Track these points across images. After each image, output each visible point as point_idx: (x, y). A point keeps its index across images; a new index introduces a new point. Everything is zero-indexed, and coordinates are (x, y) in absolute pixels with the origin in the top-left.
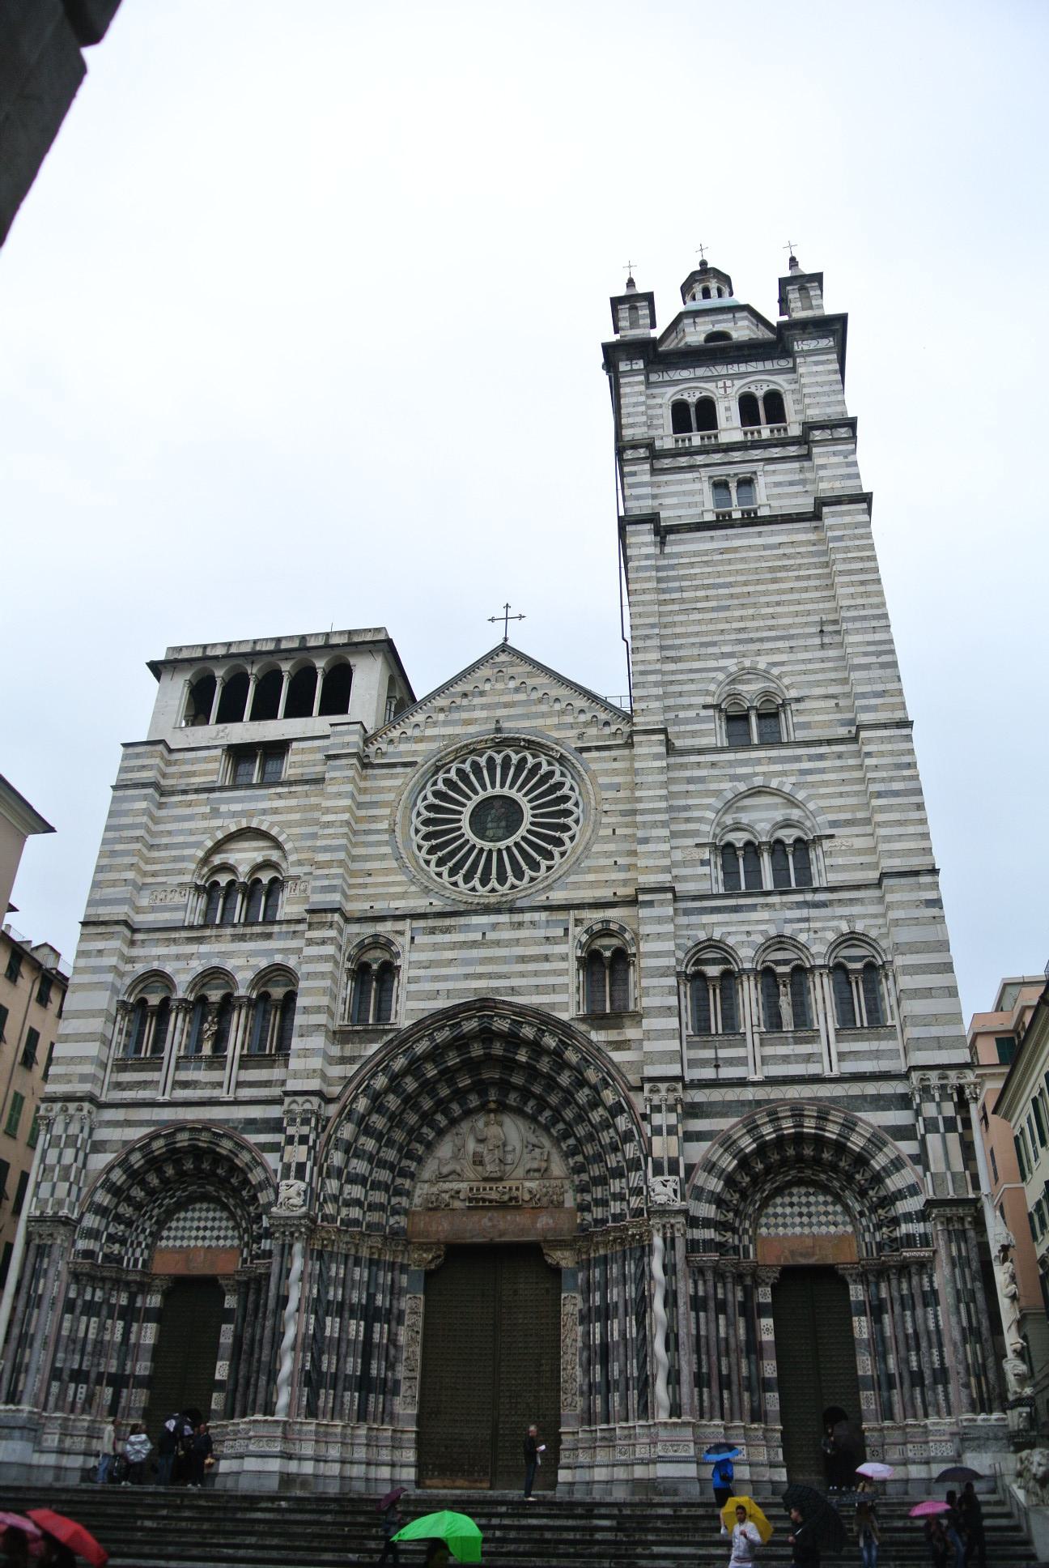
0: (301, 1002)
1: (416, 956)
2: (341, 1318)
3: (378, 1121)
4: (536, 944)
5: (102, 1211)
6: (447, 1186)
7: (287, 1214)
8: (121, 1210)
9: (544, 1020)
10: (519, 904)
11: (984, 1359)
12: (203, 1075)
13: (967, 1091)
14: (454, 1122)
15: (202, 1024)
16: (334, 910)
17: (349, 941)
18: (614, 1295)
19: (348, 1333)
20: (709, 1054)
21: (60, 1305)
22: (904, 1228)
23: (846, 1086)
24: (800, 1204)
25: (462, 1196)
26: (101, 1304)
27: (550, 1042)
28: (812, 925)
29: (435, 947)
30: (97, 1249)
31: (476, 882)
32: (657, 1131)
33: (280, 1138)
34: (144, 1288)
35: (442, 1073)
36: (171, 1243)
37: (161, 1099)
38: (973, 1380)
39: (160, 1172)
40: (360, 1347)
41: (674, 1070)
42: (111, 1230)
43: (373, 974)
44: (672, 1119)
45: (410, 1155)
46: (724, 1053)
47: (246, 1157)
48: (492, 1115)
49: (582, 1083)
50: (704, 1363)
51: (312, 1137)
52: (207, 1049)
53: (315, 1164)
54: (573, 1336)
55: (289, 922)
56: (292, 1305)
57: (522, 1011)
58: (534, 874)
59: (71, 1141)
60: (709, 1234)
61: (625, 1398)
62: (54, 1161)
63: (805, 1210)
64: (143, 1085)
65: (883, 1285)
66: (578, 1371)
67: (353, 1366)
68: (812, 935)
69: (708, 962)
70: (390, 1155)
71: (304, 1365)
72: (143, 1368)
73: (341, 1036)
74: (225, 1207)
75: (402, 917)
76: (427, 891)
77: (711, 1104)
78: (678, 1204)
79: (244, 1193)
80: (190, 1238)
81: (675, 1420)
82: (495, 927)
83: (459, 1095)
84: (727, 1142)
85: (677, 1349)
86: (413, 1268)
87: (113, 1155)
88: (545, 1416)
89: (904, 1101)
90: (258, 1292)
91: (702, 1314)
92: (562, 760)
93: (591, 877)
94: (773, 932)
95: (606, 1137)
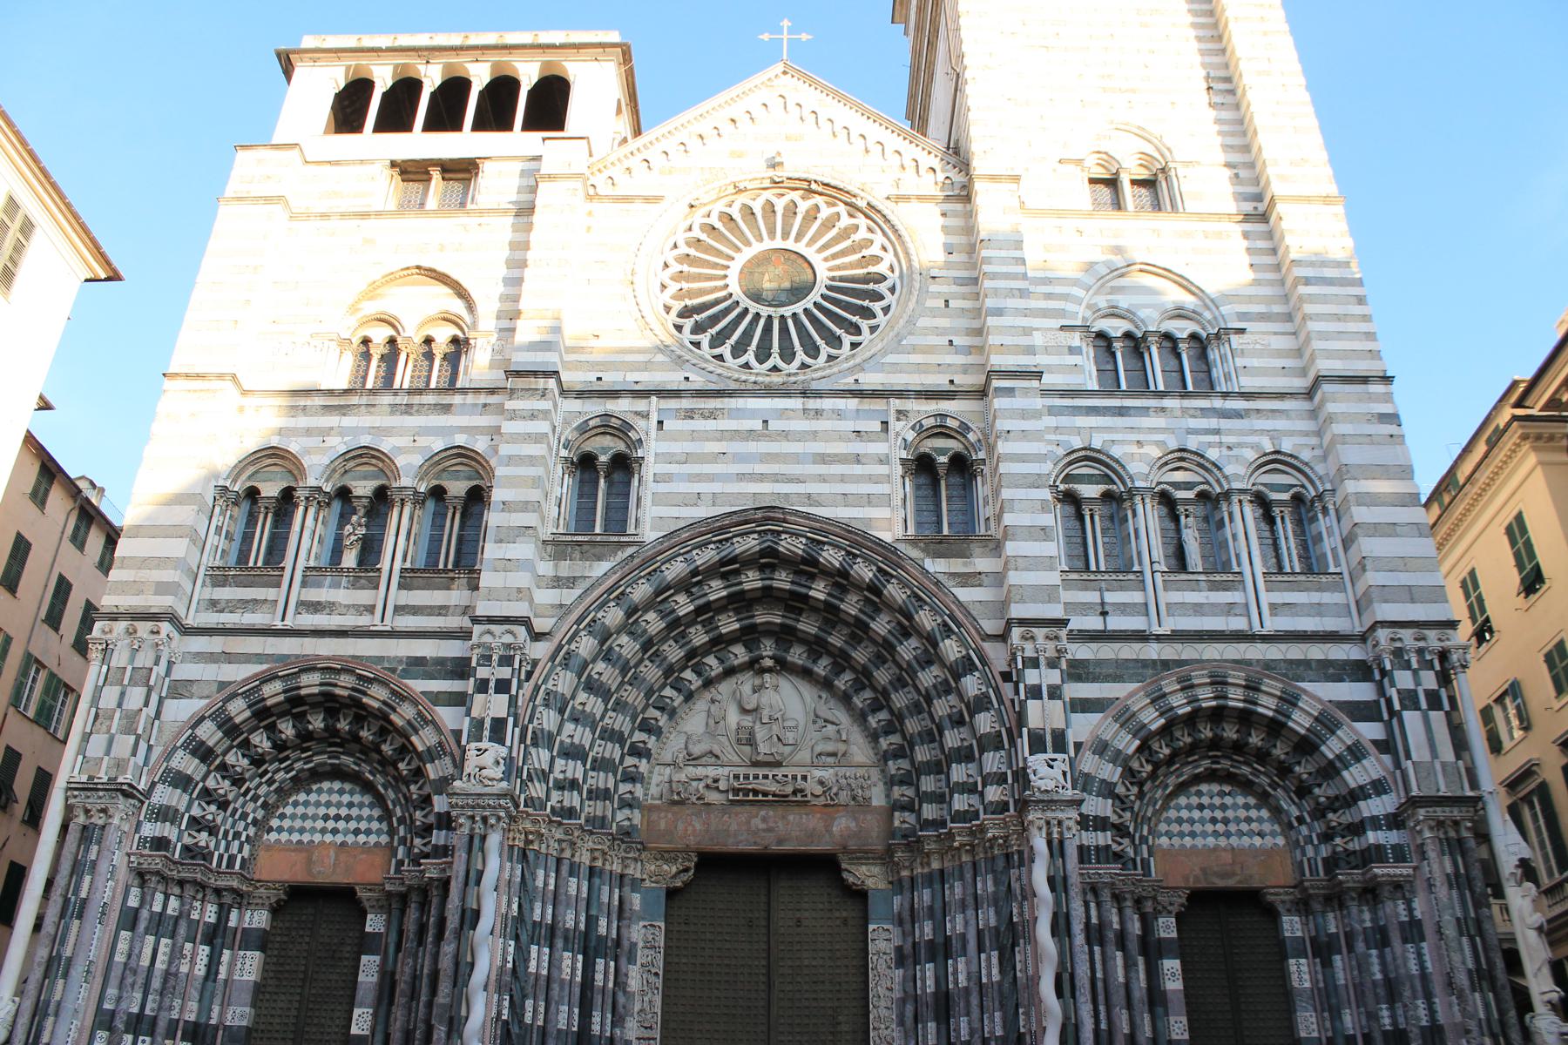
0: (497, 495)
2: (551, 947)
4: (840, 439)
5: (181, 781)
6: (700, 771)
7: (479, 789)
8: (211, 783)
9: (857, 541)
10: (814, 386)
11: (1502, 1012)
12: (343, 596)
13: (1454, 657)
14: (708, 683)
15: (341, 526)
16: (547, 374)
17: (566, 422)
18: (956, 924)
19: (560, 968)
20: (1092, 597)
21: (114, 916)
22: (1372, 837)
23: (1283, 646)
24: (1212, 807)
25: (722, 785)
26: (177, 919)
27: (864, 572)
28: (1225, 439)
29: (693, 436)
30: (174, 838)
31: (750, 357)
32: (1035, 692)
33: (469, 686)
34: (241, 899)
35: (699, 611)
36: (284, 836)
37: (279, 625)
39: (272, 729)
40: (577, 991)
41: (1056, 612)
42: (196, 811)
43: (604, 470)
44: (1054, 677)
45: (647, 727)
46: (1111, 597)
47: (407, 711)
48: (767, 676)
49: (907, 629)
50: (1103, 1016)
51: (515, 681)
52: (350, 559)
53: (515, 725)
54: (885, 983)
55: (477, 390)
57: (824, 531)
58: (833, 352)
59: (142, 677)
60: (1103, 838)
62: (113, 704)
63: (1218, 814)
64: (254, 604)
65: (1331, 916)
68: (1225, 451)
70: (621, 722)
71: (499, 1013)
73: (558, 548)
74: (368, 787)
75: (645, 394)
76: (679, 361)
77: (1099, 663)
78: (1069, 793)
79: (401, 766)
82: (783, 414)
83: (719, 643)
84: (1126, 718)
85: (1073, 996)
86: (647, 884)
87: (204, 702)
89: (1360, 671)
90: (424, 906)
91: (1097, 949)
92: (871, 212)
94: (1173, 444)
95: (941, 707)
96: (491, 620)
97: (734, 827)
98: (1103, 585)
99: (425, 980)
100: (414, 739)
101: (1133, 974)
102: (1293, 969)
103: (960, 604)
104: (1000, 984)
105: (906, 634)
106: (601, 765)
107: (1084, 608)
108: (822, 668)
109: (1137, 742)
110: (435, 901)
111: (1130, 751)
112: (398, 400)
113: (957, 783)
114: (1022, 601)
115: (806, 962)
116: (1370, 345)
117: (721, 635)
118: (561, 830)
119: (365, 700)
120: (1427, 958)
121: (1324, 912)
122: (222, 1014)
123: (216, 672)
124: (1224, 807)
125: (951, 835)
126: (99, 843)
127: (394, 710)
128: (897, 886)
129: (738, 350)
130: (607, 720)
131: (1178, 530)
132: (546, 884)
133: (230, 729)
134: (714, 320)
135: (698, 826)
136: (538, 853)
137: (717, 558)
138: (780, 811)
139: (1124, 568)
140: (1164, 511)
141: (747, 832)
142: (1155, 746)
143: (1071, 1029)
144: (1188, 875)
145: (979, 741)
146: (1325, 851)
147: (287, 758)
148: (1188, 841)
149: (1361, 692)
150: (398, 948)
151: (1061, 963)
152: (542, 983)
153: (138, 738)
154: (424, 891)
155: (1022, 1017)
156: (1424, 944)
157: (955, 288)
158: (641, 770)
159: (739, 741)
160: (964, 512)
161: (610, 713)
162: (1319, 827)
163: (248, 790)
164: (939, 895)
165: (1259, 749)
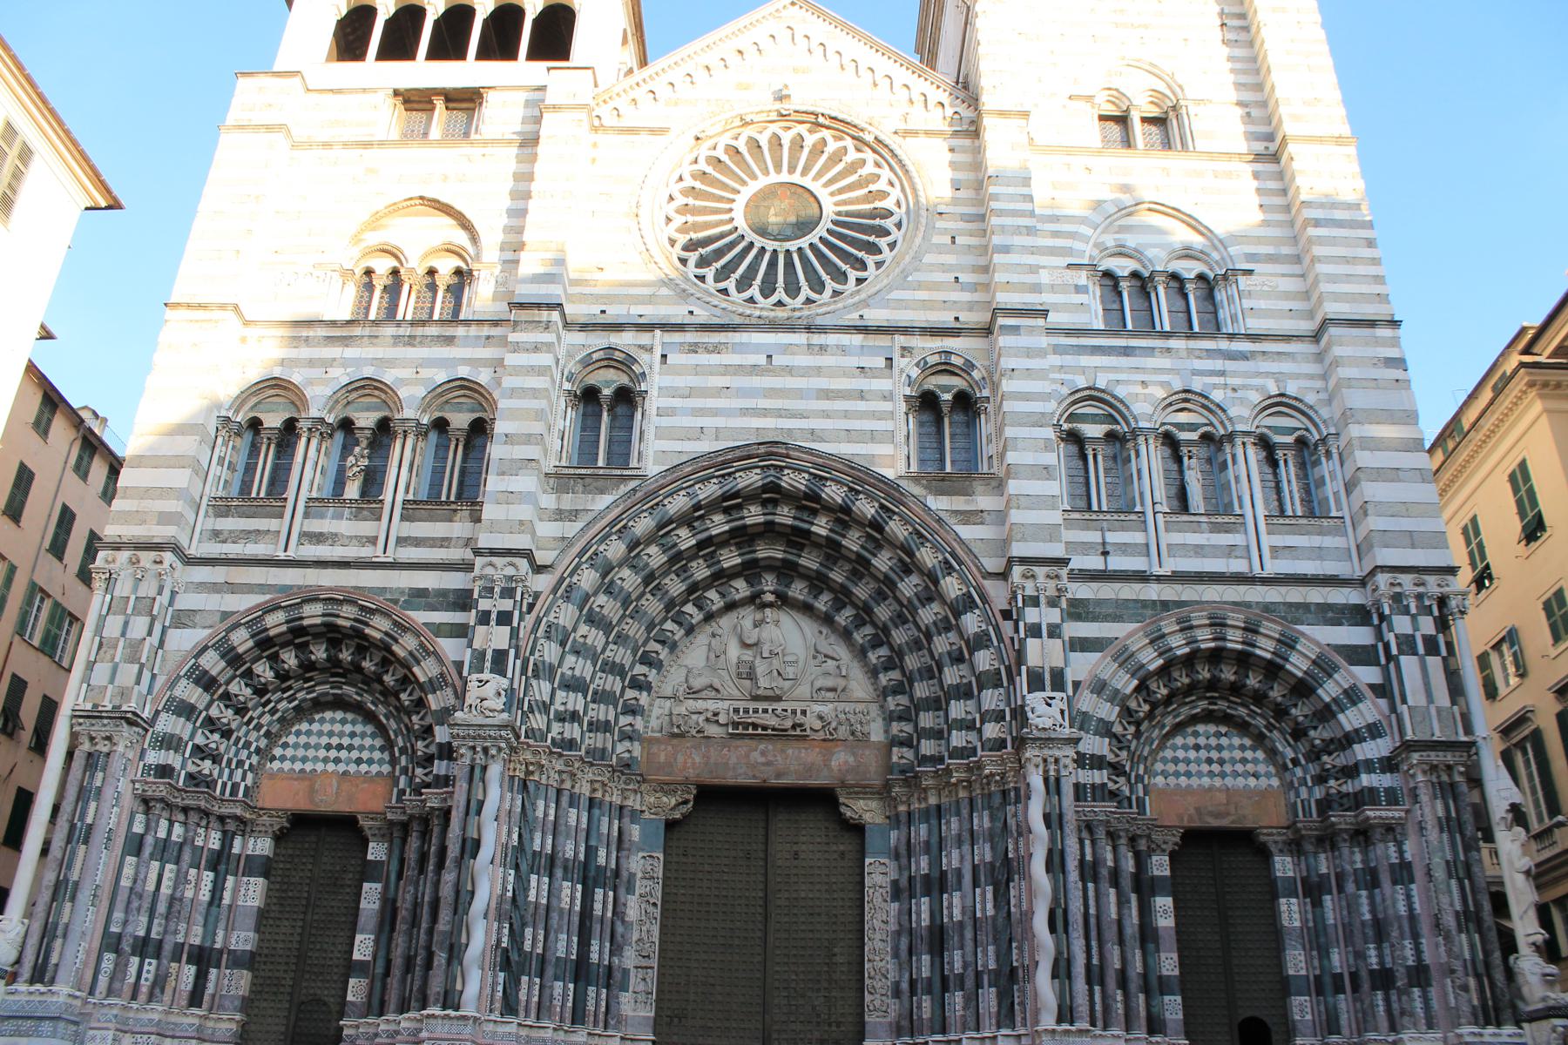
0: (500, 427)
1: (668, 381)
2: (551, 876)
3: (606, 605)
5: (185, 710)
6: (700, 705)
7: (480, 720)
9: (860, 478)
10: (819, 321)
11: (1486, 953)
12: (345, 527)
14: (709, 617)
15: (343, 458)
16: (551, 307)
17: (570, 355)
20: (1094, 537)
21: (119, 841)
22: (1366, 780)
23: (1283, 589)
24: (1208, 748)
25: (722, 719)
26: (181, 845)
28: (1230, 381)
29: (697, 370)
30: (177, 766)
31: (754, 291)
32: (1035, 631)
33: (471, 617)
34: (244, 826)
35: (701, 545)
37: (282, 555)
38: (1472, 982)
39: (274, 659)
40: (576, 919)
41: (1057, 551)
42: (199, 740)
44: (1054, 616)
45: (647, 660)
46: (1111, 537)
48: (768, 611)
50: (1095, 951)
51: (516, 614)
52: (352, 491)
53: (516, 657)
54: (881, 916)
55: (480, 322)
56: (486, 852)
57: (826, 467)
58: (839, 287)
59: (146, 606)
60: (1100, 777)
61: (972, 1001)
62: (117, 633)
63: (1214, 755)
65: (1322, 856)
66: (890, 965)
67: (564, 946)
68: (1230, 393)
69: (1084, 418)
70: (622, 655)
71: (499, 941)
72: (243, 939)
73: (561, 481)
74: (370, 717)
75: (649, 327)
76: (684, 295)
77: (1099, 602)
78: (1067, 732)
80: (316, 759)
81: (1065, 1026)
82: (787, 349)
83: (721, 577)
84: (1124, 658)
85: (1066, 931)
86: (647, 815)
87: (207, 632)
88: (838, 1024)
89: (1359, 615)
90: (425, 834)
91: (1090, 885)
92: (879, 146)
93: (922, 295)
94: (1178, 385)
95: (941, 644)
96: (493, 552)
97: (733, 760)
98: (1105, 524)
99: (426, 908)
100: (416, 670)
101: (1126, 911)
102: (1284, 908)
103: (961, 541)
104: (994, 918)
105: (907, 570)
106: (601, 697)
107: (1085, 548)
108: (823, 603)
109: (1135, 682)
110: (436, 831)
111: (1128, 690)
112: (401, 331)
113: (955, 720)
114: (1023, 539)
115: (803, 895)
116: (1377, 289)
117: (723, 570)
118: (561, 761)
119: (367, 631)
120: (1416, 899)
121: (1316, 853)
122: (226, 937)
123: (219, 602)
124: (1219, 748)
125: (948, 772)
126: (104, 770)
127: (396, 641)
128: (894, 821)
129: (743, 284)
130: (608, 653)
131: (1181, 472)
132: (546, 815)
133: (233, 659)
134: (719, 253)
135: (697, 760)
136: (537, 784)
137: (720, 492)
138: (779, 745)
139: (1126, 509)
140: (1168, 452)
141: (746, 765)
142: (1153, 686)
143: (1063, 964)
144: (1184, 815)
145: (978, 678)
146: (1318, 793)
147: (290, 688)
148: (1183, 780)
149: (1359, 636)
150: (400, 876)
151: (1055, 899)
152: (542, 912)
153: (142, 666)
154: (425, 821)
155: (1015, 951)
156: (1413, 886)
157: (962, 225)
158: (642, 702)
159: (739, 676)
160: (967, 450)
161: (611, 646)
162: (1313, 769)
163: (251, 719)
164: (936, 830)
165: (1256, 691)
